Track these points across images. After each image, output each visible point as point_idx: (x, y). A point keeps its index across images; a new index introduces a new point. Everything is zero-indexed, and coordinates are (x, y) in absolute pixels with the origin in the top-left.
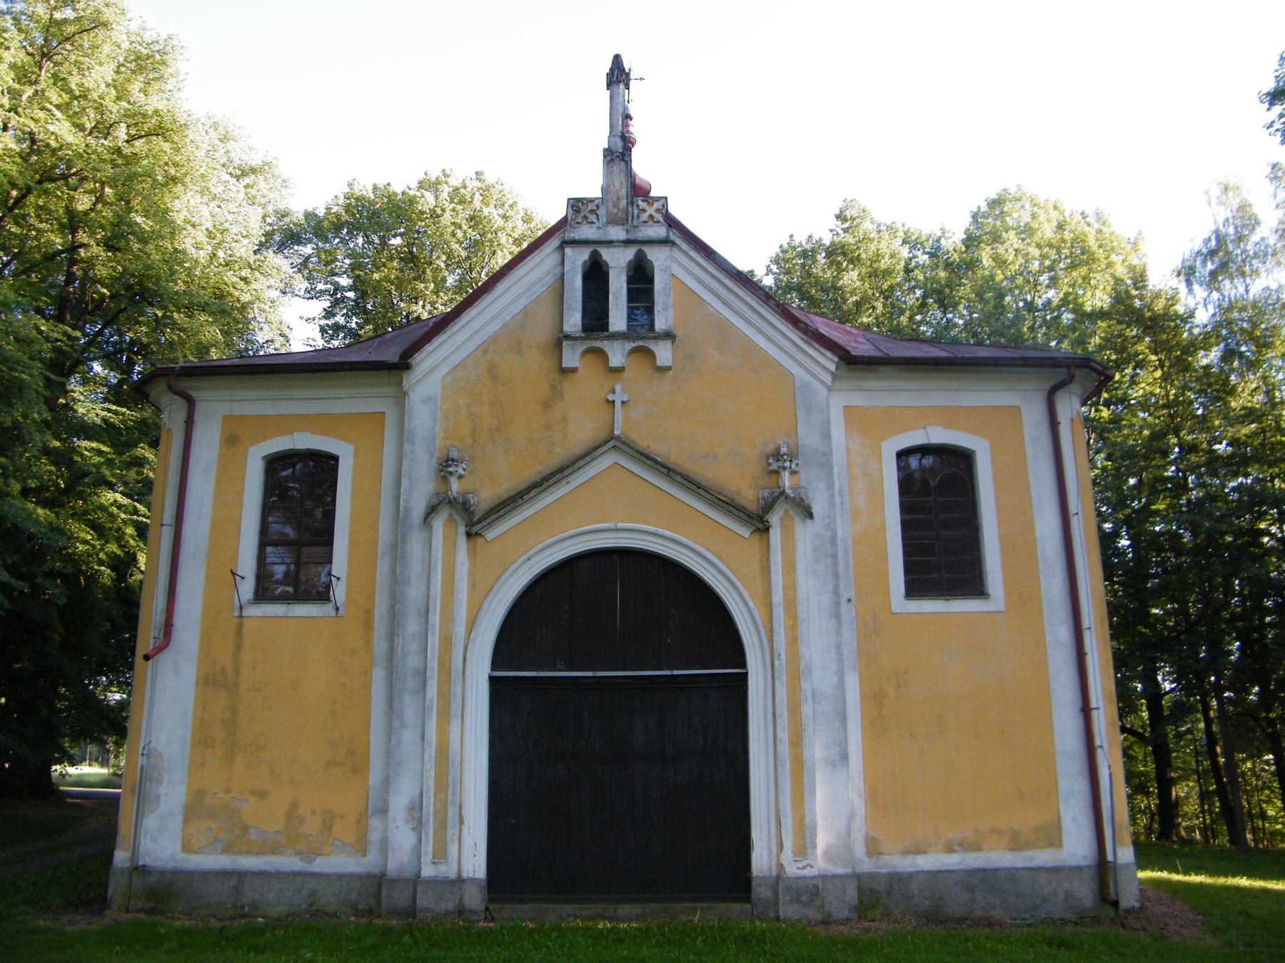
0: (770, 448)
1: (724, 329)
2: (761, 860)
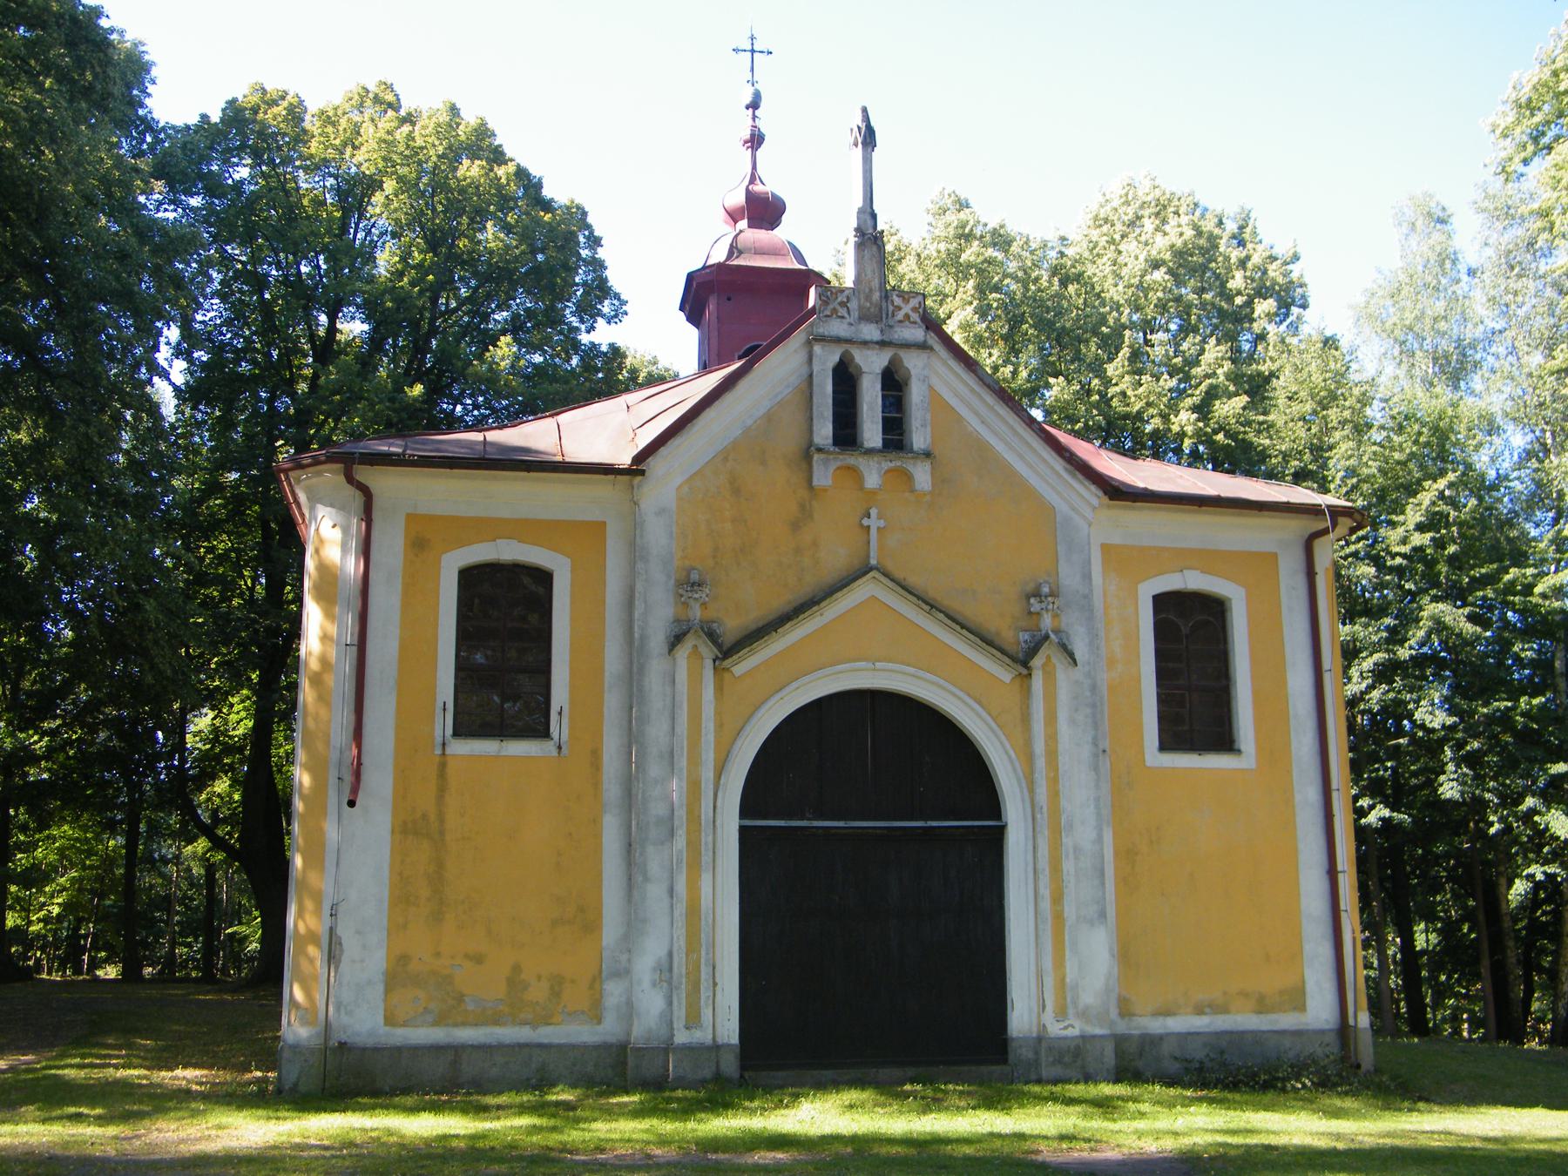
0: (1030, 587)
1: (982, 450)
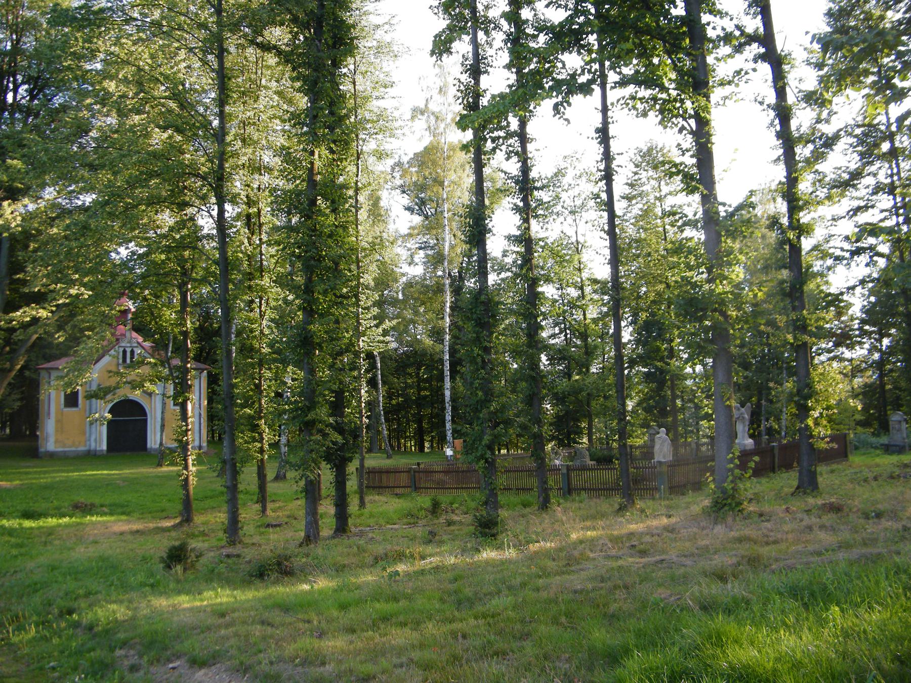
2: (149, 446)
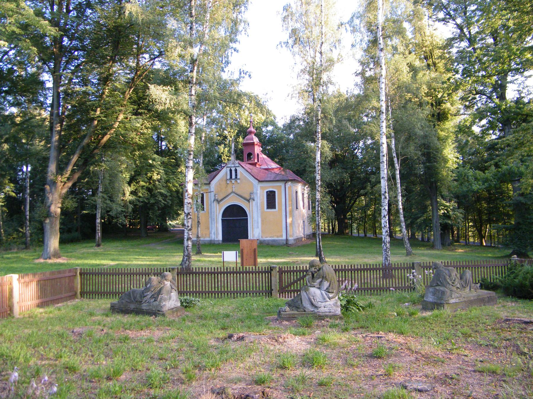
1: (246, 177)
